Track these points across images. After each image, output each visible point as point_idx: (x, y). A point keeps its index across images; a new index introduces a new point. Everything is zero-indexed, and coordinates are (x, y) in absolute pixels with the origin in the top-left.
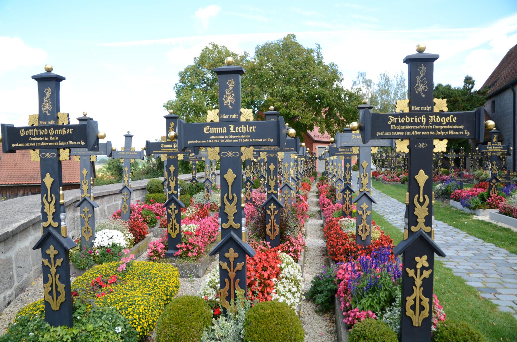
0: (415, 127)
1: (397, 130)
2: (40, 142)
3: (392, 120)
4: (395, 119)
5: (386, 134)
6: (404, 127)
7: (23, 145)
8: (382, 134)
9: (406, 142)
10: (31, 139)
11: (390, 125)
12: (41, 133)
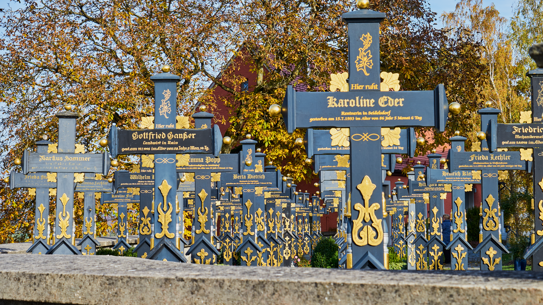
0: (537, 137)
1: (521, 140)
2: (156, 146)
3: (516, 130)
4: (519, 129)
5: (511, 143)
6: (527, 137)
7: (135, 149)
8: (507, 143)
9: (530, 151)
10: (145, 143)
11: (514, 135)
12: (158, 137)
